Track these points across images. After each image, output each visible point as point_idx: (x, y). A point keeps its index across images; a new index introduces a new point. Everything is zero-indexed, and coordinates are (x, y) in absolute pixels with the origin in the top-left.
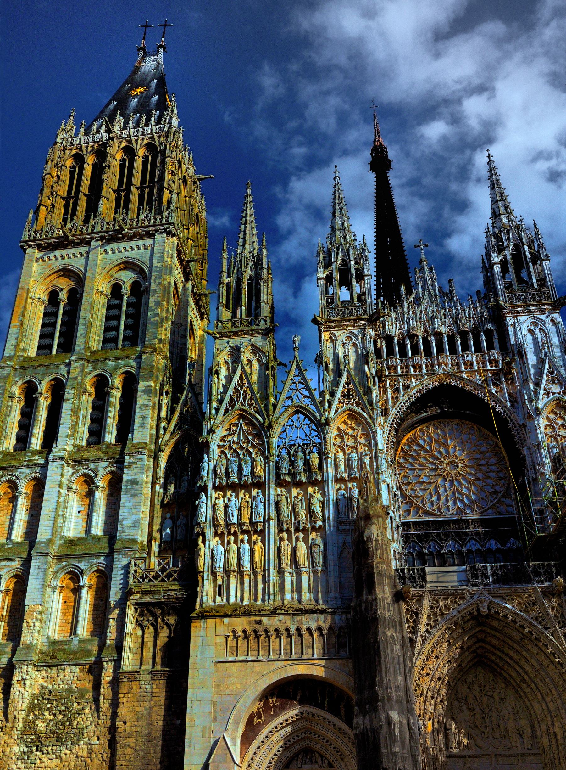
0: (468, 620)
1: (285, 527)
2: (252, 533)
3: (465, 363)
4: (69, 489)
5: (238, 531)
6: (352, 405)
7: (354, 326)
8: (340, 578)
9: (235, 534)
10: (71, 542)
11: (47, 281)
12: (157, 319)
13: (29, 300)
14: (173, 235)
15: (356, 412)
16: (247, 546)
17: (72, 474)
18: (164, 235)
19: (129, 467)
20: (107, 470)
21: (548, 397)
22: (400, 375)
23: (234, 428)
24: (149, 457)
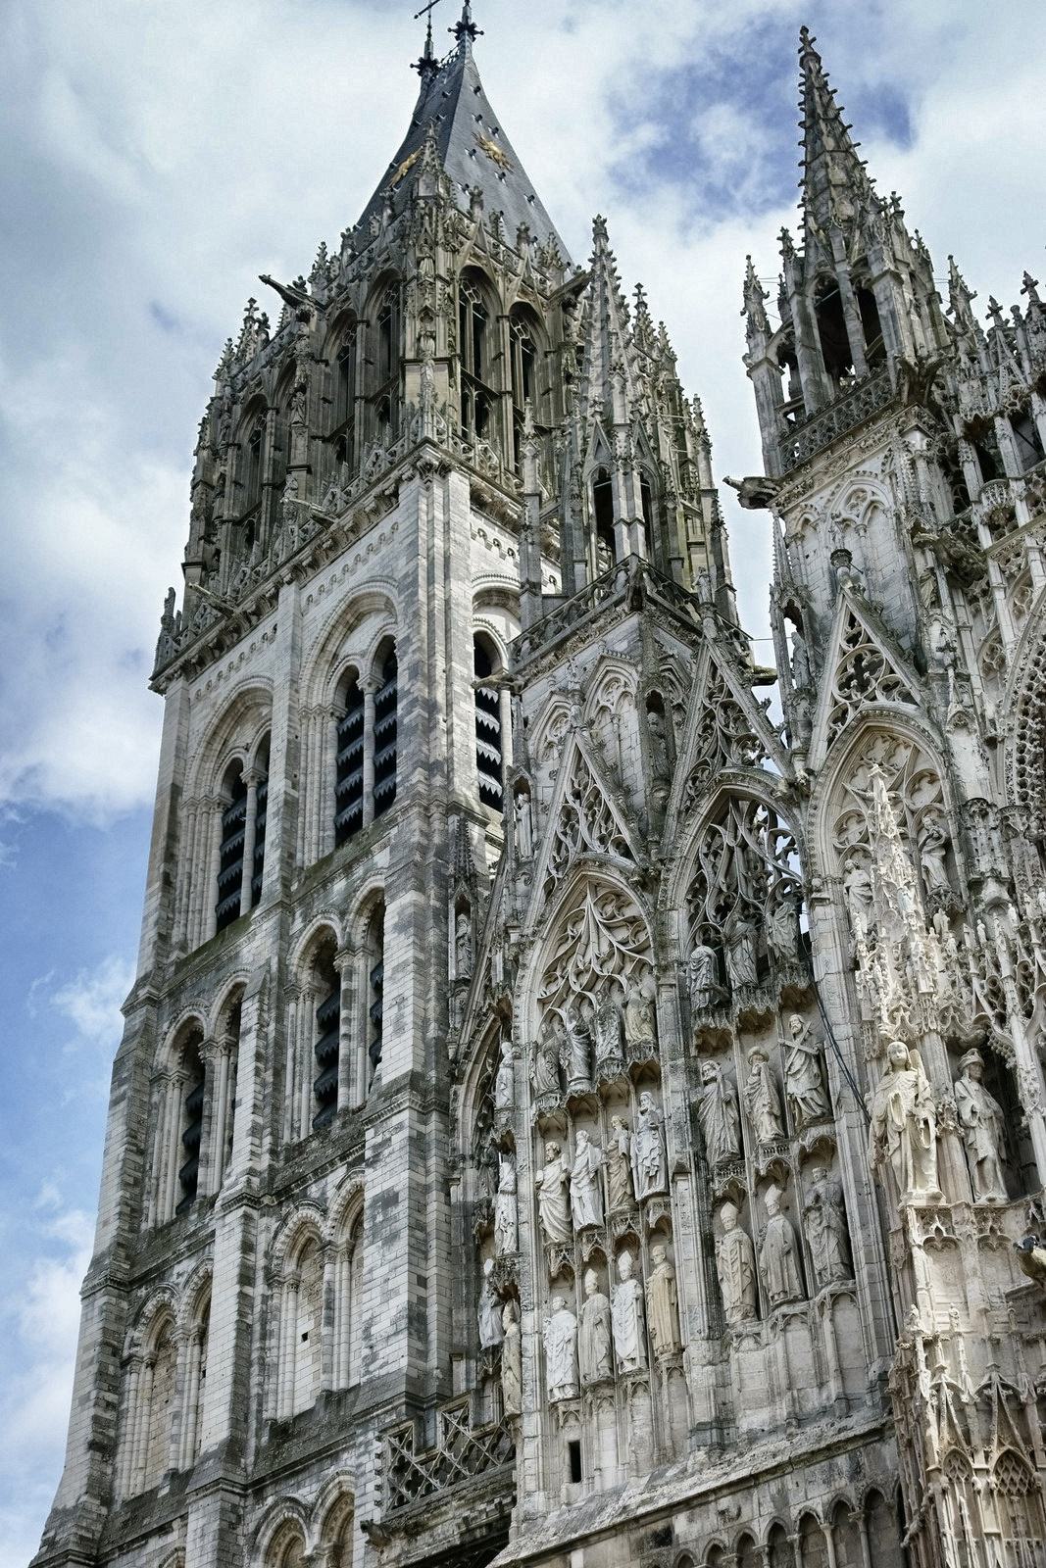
1: (719, 1186)
2: (643, 1241)
4: (271, 1279)
5: (608, 1249)
7: (863, 450)
9: (597, 1260)
10: (282, 1432)
11: (217, 746)
12: (417, 711)
13: (182, 813)
14: (444, 470)
15: (882, 712)
16: (628, 1291)
17: (275, 1237)
18: (417, 480)
19: (373, 1163)
20: (343, 1192)
23: (582, 927)
24: (423, 1114)
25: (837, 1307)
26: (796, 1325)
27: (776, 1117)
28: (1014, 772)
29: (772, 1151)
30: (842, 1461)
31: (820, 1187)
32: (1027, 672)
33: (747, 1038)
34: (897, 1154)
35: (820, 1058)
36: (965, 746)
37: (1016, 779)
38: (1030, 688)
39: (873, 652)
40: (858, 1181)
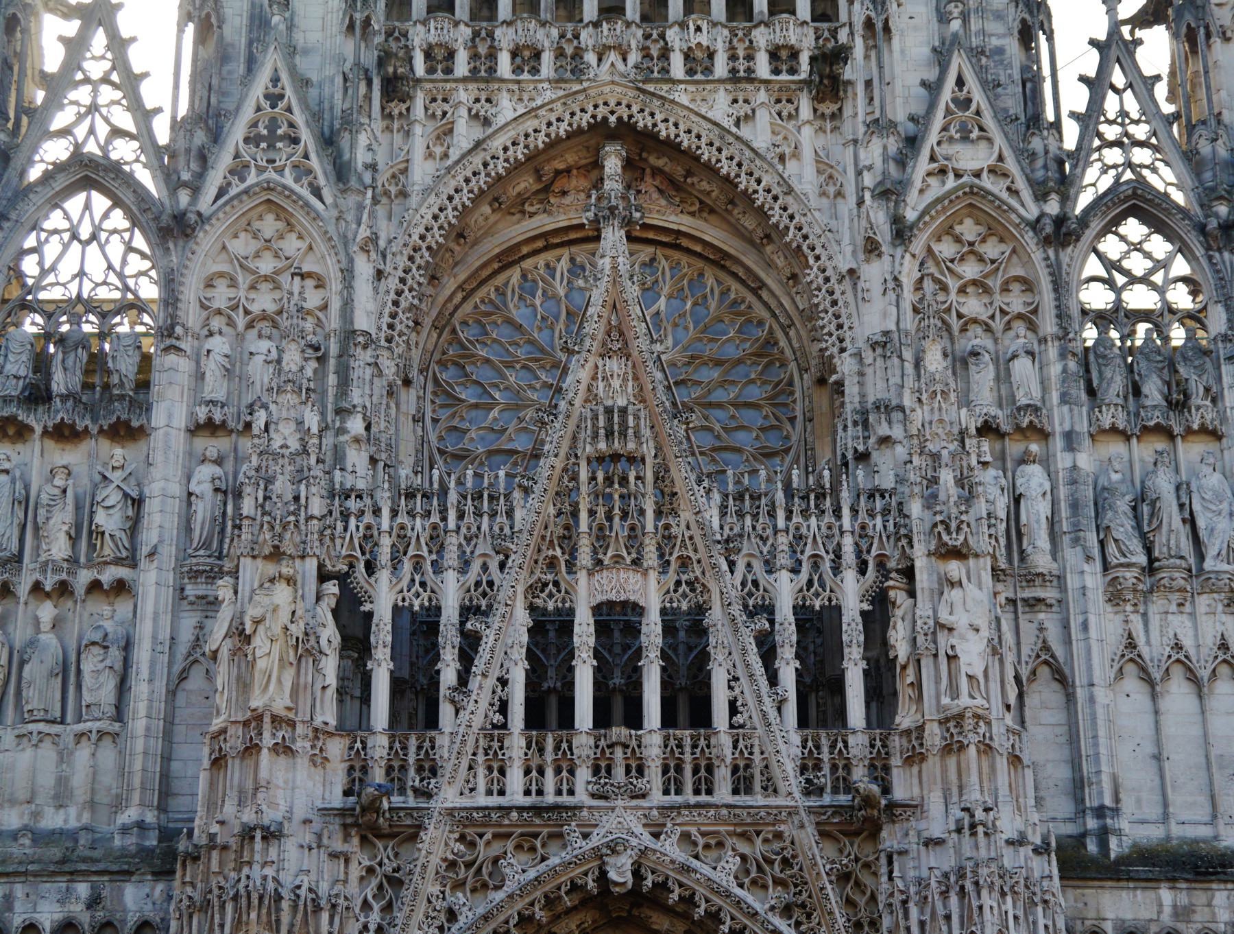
0: (569, 912)
3: (688, 56)
6: (280, 171)
8: (167, 759)
21: (944, 183)
22: (464, 80)
25: (100, 743)
26: (47, 744)
27: (70, 537)
28: (387, 311)
29: (61, 570)
30: (83, 889)
31: (108, 625)
32: (424, 221)
33: (50, 444)
34: (266, 658)
35: (138, 503)
36: (364, 268)
37: (386, 319)
38: (422, 238)
39: (292, 125)
40: (154, 637)
